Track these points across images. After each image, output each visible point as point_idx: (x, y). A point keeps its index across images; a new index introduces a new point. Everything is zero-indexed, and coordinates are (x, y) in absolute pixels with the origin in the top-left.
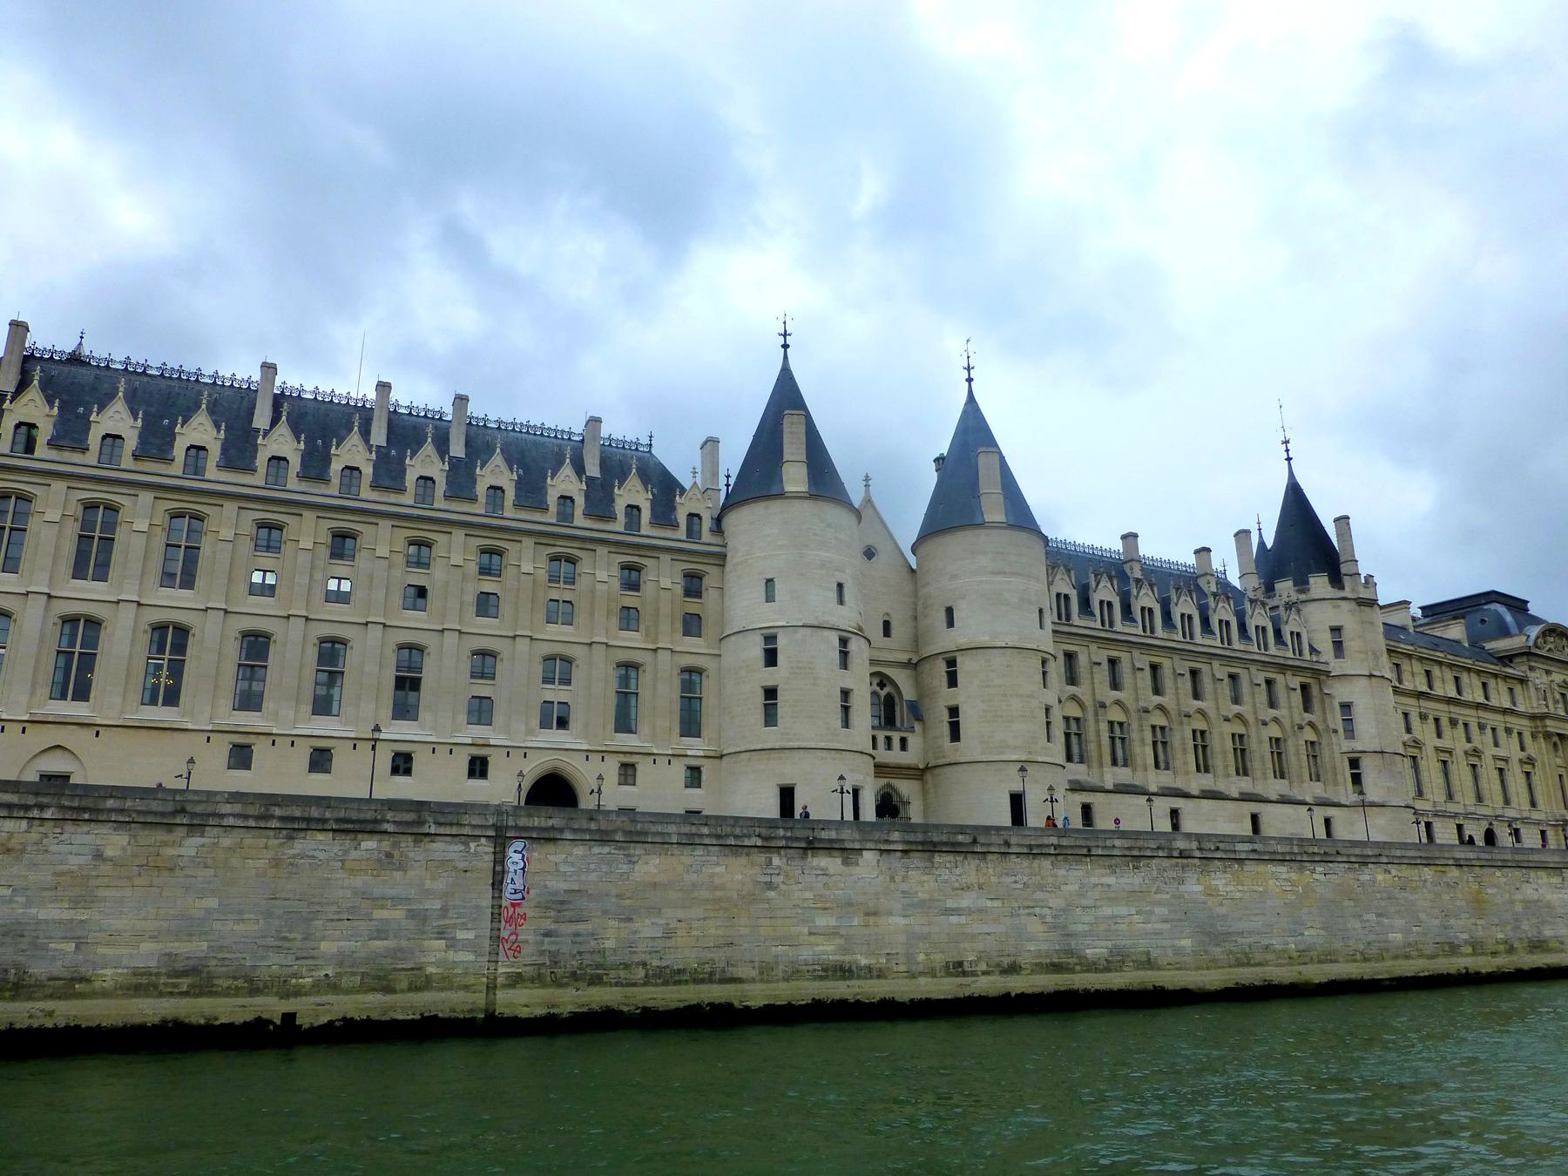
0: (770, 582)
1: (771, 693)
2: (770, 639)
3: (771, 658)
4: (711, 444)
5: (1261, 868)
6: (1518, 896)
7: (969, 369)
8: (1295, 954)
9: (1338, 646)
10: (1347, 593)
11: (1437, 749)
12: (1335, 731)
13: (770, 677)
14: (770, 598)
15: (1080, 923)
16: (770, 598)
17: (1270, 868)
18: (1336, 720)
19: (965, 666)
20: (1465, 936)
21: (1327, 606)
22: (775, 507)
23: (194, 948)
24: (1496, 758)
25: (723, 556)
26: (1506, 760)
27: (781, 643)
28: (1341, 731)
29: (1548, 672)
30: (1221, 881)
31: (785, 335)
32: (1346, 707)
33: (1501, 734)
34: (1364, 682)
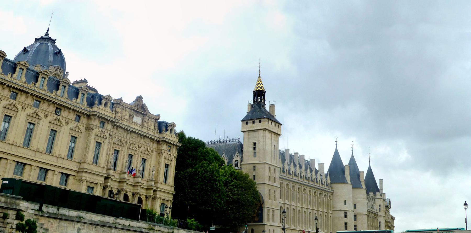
0: (345, 201)
1: (346, 223)
2: (346, 213)
3: (346, 217)
4: (321, 165)
7: (352, 148)
9: (380, 208)
10: (382, 197)
13: (346, 220)
14: (345, 204)
16: (345, 204)
18: (378, 225)
19: (359, 217)
21: (379, 200)
22: (346, 185)
25: (333, 193)
27: (348, 214)
31: (336, 142)
32: (380, 223)
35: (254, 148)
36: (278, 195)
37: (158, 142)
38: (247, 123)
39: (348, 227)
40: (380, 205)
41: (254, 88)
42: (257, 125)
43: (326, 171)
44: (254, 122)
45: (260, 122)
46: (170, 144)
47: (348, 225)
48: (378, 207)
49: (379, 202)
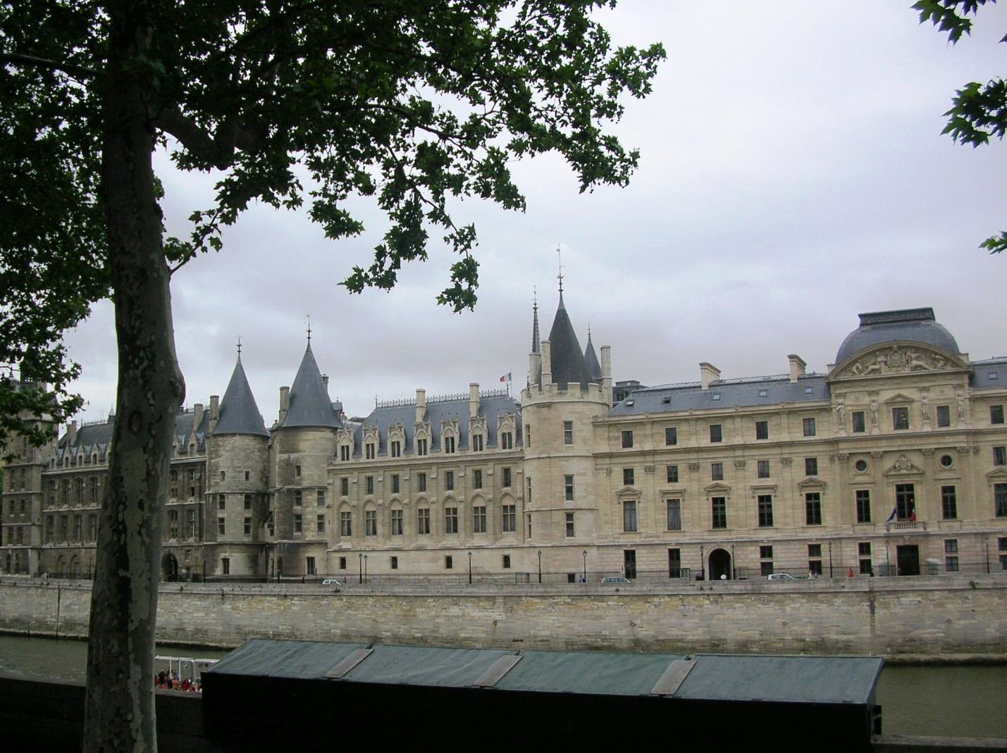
5: (263, 598)
6: (444, 613)
8: (271, 636)
11: (665, 493)
12: (523, 499)
15: (186, 619)
17: (268, 598)
20: (389, 634)
23: (16, 615)
24: (755, 488)
26: (773, 488)
28: (526, 497)
29: (870, 393)
30: (241, 604)
33: (774, 467)
34: (535, 463)
40: (528, 427)
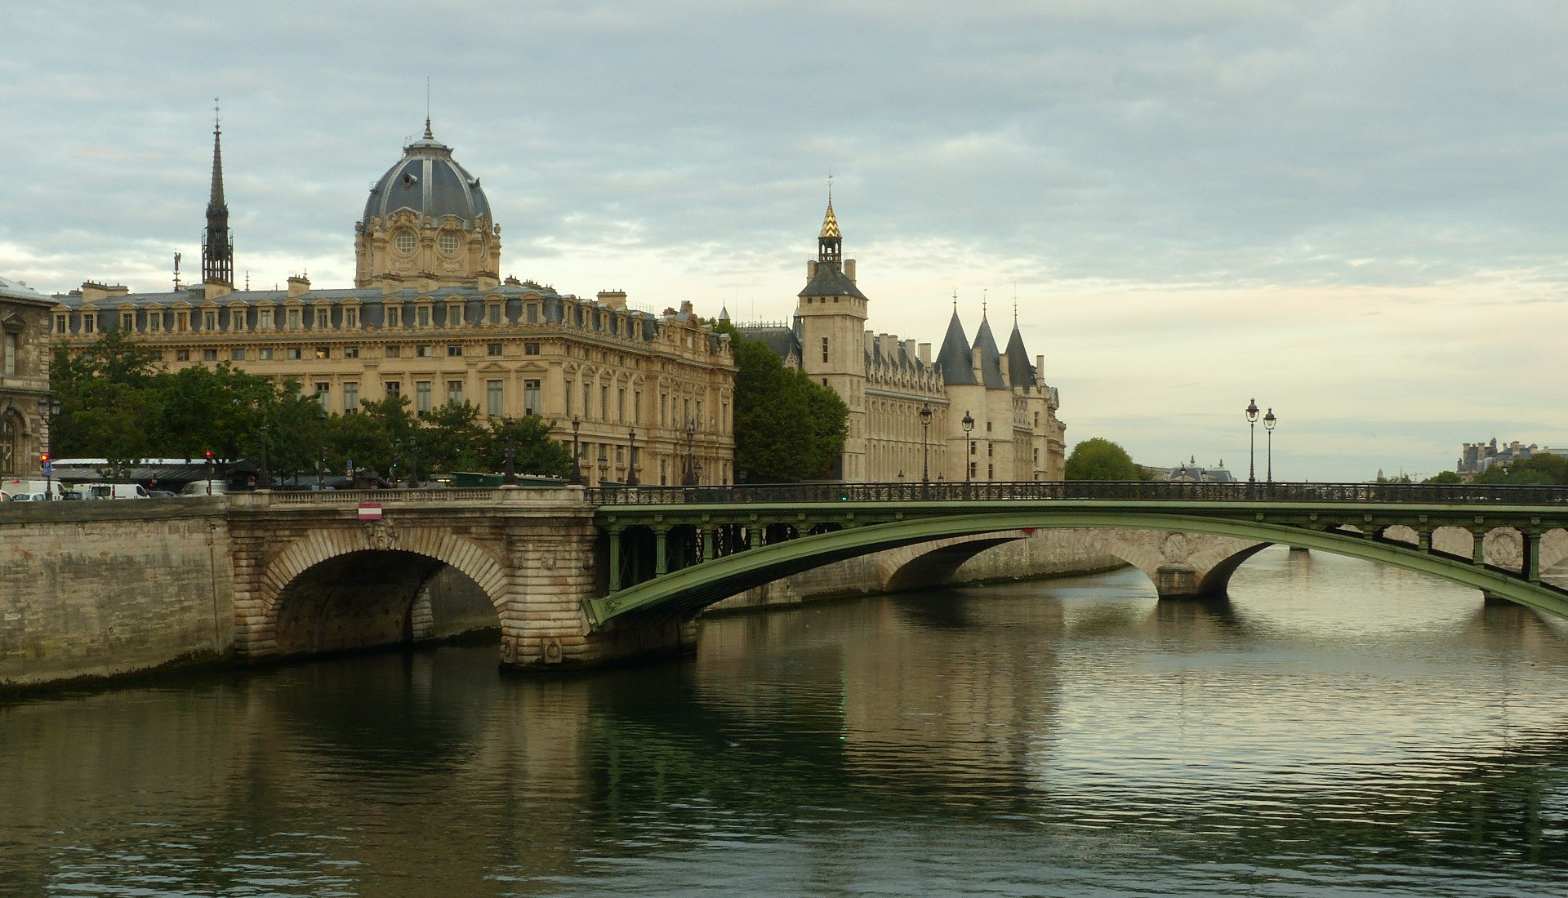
13: (972, 458)
19: (997, 448)
35: (825, 349)
36: (862, 428)
37: (712, 372)
38: (810, 301)
39: (978, 472)
41: (817, 230)
42: (830, 307)
43: (934, 359)
44: (823, 301)
45: (836, 300)
46: (725, 372)
47: (978, 467)
48: (1033, 416)
49: (1036, 406)
